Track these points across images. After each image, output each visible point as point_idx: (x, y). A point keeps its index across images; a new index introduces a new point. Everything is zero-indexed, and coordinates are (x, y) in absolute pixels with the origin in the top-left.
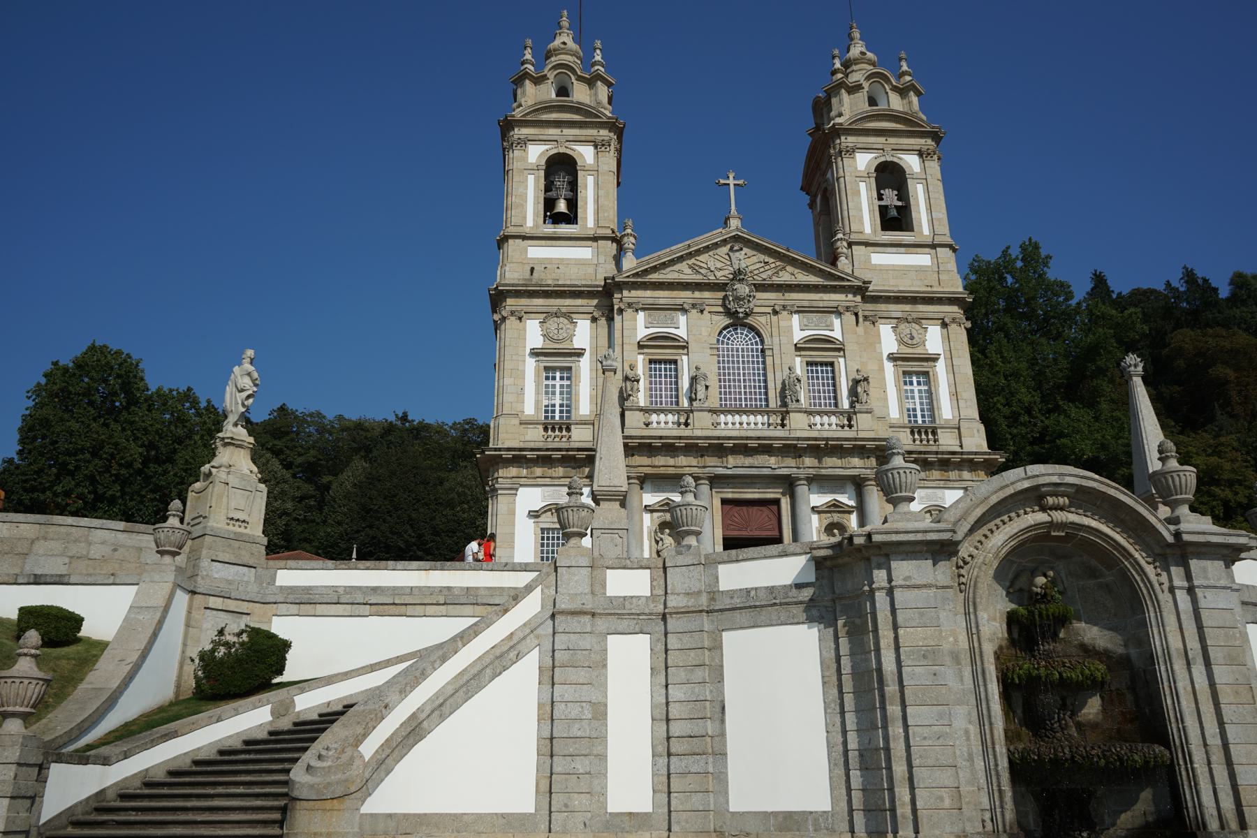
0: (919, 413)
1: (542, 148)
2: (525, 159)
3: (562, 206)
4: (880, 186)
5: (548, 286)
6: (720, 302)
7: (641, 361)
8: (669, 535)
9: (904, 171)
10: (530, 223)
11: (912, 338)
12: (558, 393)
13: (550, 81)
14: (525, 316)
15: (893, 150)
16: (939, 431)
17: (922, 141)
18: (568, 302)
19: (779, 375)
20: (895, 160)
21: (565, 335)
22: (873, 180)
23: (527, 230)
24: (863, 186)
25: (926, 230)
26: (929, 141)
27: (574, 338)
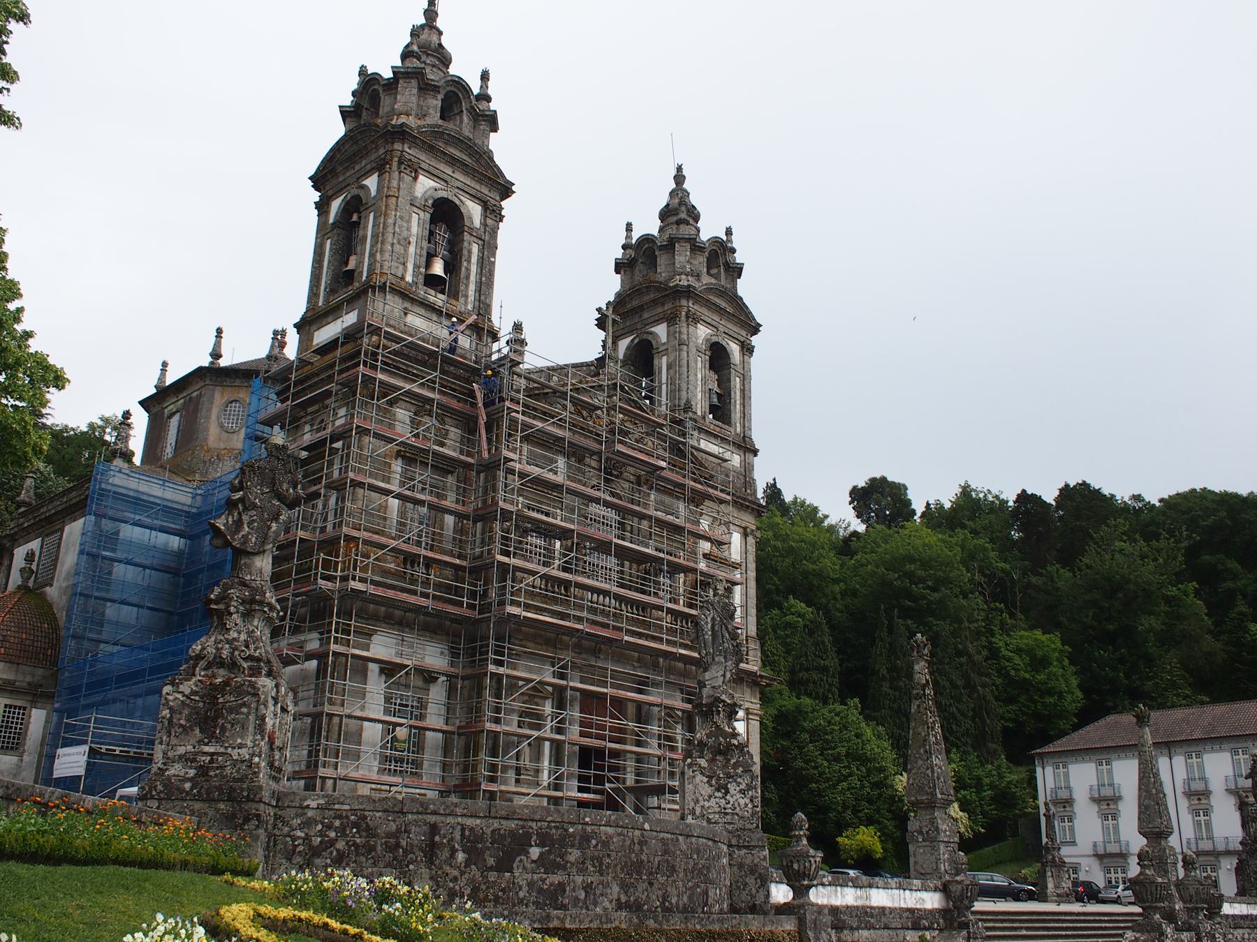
2: (411, 189)
10: (409, 278)
17: (744, 333)
20: (724, 344)
22: (707, 358)
25: (738, 430)
26: (749, 335)
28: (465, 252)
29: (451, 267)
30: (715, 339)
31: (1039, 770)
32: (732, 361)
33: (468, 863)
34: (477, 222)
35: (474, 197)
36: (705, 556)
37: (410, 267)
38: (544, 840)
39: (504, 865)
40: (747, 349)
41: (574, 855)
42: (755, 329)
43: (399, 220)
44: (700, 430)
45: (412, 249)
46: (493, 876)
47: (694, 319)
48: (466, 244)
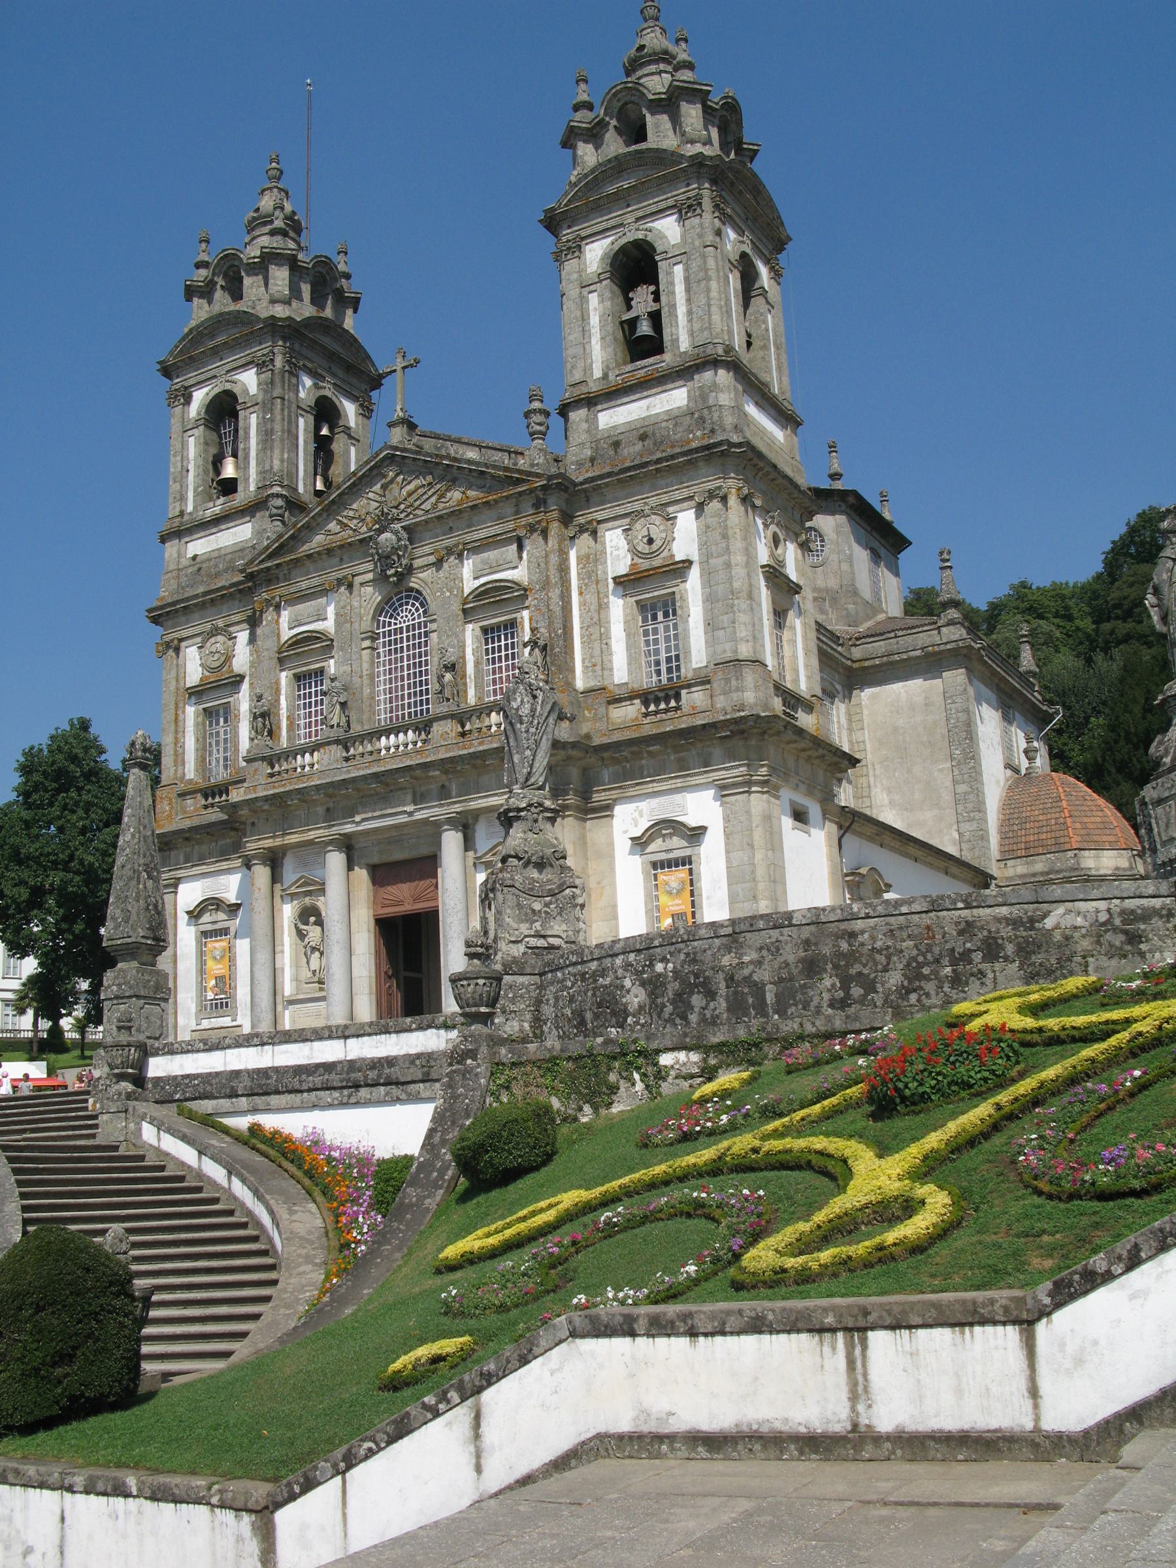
0: (663, 667)
1: (206, 390)
3: (229, 470)
5: (196, 596)
6: (370, 566)
8: (316, 923)
9: (654, 249)
10: (190, 508)
11: (651, 541)
12: (222, 744)
13: (218, 287)
14: (184, 644)
15: (638, 219)
16: (684, 692)
20: (641, 237)
21: (223, 659)
24: (594, 299)
28: (241, 432)
30: (616, 247)
32: (659, 249)
35: (245, 366)
37: (191, 495)
44: (590, 402)
47: (576, 248)
48: (241, 423)
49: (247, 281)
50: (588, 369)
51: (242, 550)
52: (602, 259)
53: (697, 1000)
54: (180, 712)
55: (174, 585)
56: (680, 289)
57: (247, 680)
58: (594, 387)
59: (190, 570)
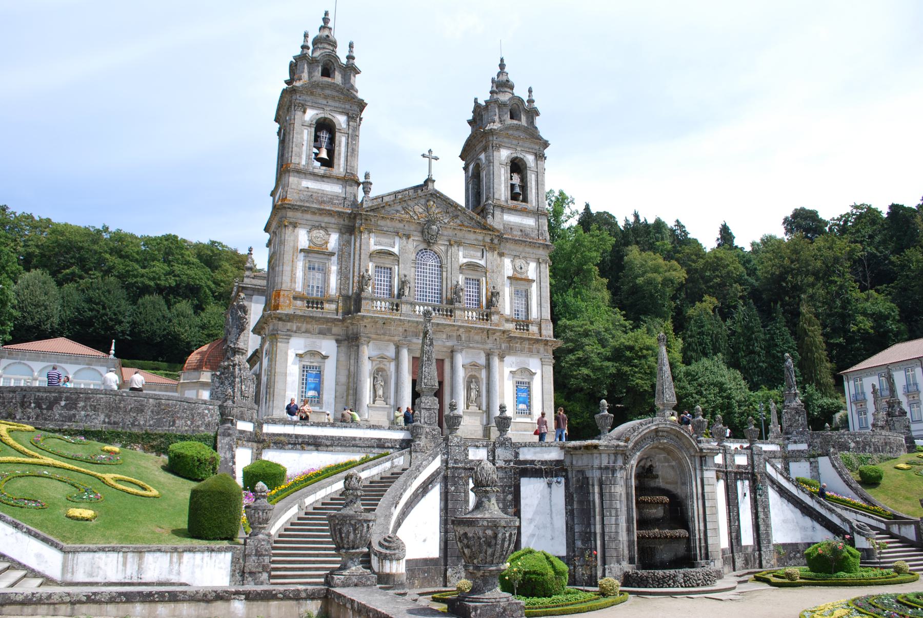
4: (512, 171)
7: (371, 266)
10: (303, 162)
11: (521, 268)
17: (537, 147)
18: (327, 219)
19: (449, 282)
20: (522, 157)
21: (323, 242)
22: (509, 167)
23: (302, 167)
24: (503, 171)
25: (534, 204)
26: (541, 149)
27: (328, 245)
28: (337, 142)
29: (331, 152)
31: (846, 383)
33: (35, 407)
34: (344, 126)
35: (341, 113)
36: (509, 278)
38: (67, 399)
39: (50, 408)
40: (540, 157)
41: (81, 404)
42: (546, 144)
43: (295, 135)
45: (304, 148)
46: (45, 412)
47: (498, 147)
49: (337, 73)
50: (500, 195)
51: (337, 196)
52: (508, 157)
53: (867, 447)
54: (295, 257)
55: (296, 196)
56: (534, 183)
57: (336, 255)
58: (503, 203)
59: (305, 193)
